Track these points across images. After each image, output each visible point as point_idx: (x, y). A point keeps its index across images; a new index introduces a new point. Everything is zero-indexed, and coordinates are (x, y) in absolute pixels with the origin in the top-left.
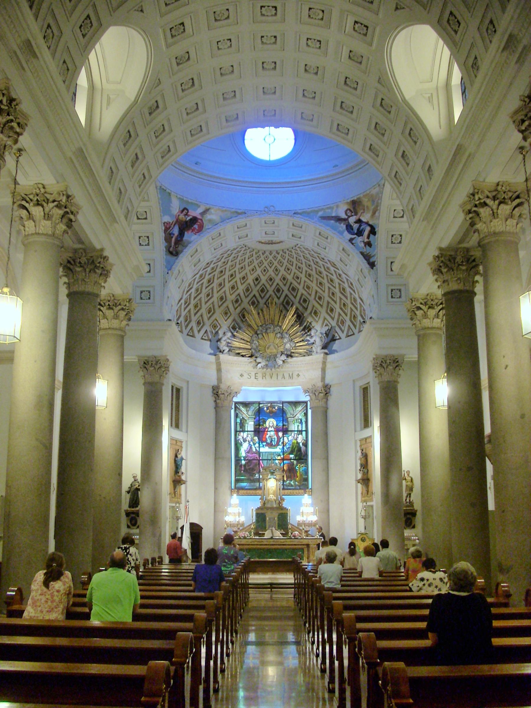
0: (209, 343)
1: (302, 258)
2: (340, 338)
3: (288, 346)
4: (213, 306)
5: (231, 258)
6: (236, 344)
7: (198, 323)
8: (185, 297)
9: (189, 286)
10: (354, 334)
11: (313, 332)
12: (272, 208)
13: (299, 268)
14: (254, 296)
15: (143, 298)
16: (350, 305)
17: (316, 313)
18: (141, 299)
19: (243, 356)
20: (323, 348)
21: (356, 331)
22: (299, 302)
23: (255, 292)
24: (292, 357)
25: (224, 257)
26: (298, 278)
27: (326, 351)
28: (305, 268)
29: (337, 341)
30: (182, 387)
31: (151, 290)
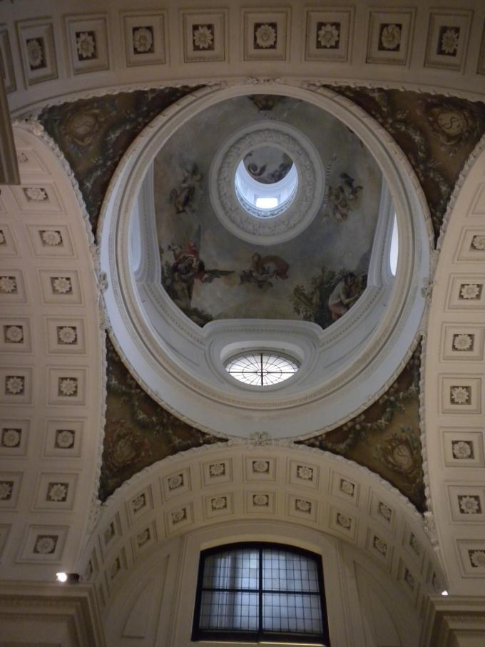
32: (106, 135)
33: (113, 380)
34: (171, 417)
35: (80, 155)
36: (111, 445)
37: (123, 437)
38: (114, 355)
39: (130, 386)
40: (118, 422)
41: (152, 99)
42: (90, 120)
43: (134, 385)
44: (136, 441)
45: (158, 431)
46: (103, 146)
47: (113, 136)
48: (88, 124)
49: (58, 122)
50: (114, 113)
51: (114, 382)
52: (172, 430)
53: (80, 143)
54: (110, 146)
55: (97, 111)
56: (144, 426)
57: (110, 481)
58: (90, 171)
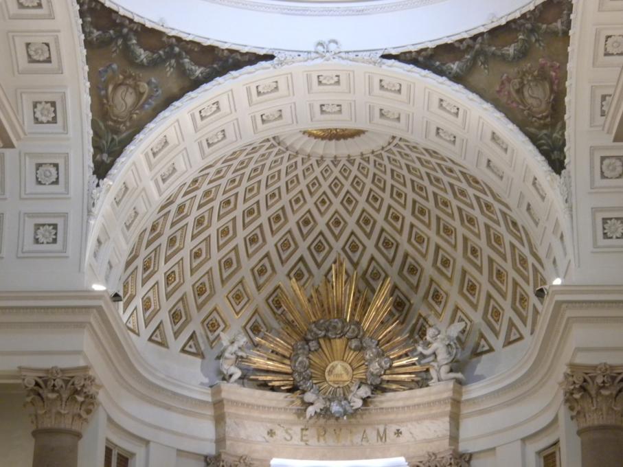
0: (198, 360)
1: (405, 172)
2: (491, 350)
3: (375, 367)
4: (211, 279)
5: (247, 171)
6: (260, 362)
7: (175, 316)
8: (144, 253)
9: (154, 228)
10: (521, 338)
11: (430, 332)
12: (332, 47)
13: (399, 195)
14: (301, 259)
15: (42, 240)
16: (513, 274)
17: (436, 296)
18: (37, 241)
19: (273, 389)
20: (451, 371)
21: (525, 331)
22: (400, 273)
23: (303, 250)
24: (384, 391)
25: (232, 169)
26: (396, 218)
27: (459, 375)
28: (411, 196)
29: (484, 357)
30: (133, 455)
31: (59, 222)
32: (141, 66)
33: (452, 66)
34: (528, 16)
35: (160, 92)
36: (521, 107)
37: (522, 85)
38: (423, 53)
39: (470, 47)
40: (503, 83)
41: (98, 30)
42: (122, 90)
43: (471, 42)
44: (536, 73)
45: (537, 40)
46: (155, 64)
47: (142, 57)
48: (124, 94)
49: (115, 137)
50: (115, 66)
51: (455, 67)
52: (543, 23)
53: (145, 96)
54: (155, 56)
55: (110, 88)
56: (523, 54)
57: (555, 135)
58: (182, 72)
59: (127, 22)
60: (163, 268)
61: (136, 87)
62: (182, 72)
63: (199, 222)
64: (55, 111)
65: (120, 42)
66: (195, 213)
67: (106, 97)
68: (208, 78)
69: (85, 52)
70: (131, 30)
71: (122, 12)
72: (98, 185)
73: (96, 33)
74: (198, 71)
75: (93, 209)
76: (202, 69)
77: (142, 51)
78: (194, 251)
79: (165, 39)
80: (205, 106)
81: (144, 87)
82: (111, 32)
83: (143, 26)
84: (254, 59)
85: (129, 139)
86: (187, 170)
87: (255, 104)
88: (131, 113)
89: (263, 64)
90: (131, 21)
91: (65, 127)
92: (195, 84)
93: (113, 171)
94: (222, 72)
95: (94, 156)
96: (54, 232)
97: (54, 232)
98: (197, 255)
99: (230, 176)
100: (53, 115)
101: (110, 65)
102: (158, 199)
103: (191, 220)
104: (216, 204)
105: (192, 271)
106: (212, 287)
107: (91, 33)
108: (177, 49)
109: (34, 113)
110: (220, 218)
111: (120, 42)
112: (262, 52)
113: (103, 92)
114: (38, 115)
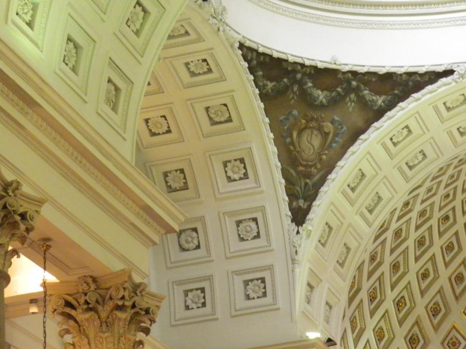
4: (443, 298)
8: (366, 285)
9: (373, 258)
15: (252, 295)
18: (248, 297)
25: (443, 185)
31: (266, 275)
32: (322, 106)
35: (345, 128)
41: (271, 81)
42: (305, 136)
46: (335, 102)
47: (321, 97)
48: (309, 137)
49: (308, 181)
50: (295, 112)
53: (331, 135)
54: (334, 94)
55: (295, 134)
58: (363, 103)
59: (299, 67)
60: (391, 296)
61: (320, 129)
62: (363, 103)
63: (420, 242)
64: (245, 168)
65: (296, 88)
66: (414, 236)
67: (292, 143)
68: (391, 106)
69: (262, 105)
70: (304, 74)
71: (291, 59)
72: (298, 232)
73: (270, 85)
74: (380, 101)
75: (296, 258)
76: (383, 97)
77: (320, 92)
78: (421, 272)
79: (340, 76)
80: (395, 132)
81: (328, 127)
82: (285, 80)
83: (315, 68)
84: (434, 77)
85: (323, 181)
86: (394, 199)
87: (447, 120)
88: (320, 155)
89: (444, 80)
90: (303, 65)
91: (257, 180)
92: (380, 114)
93: (310, 216)
94: (404, 97)
95: (290, 205)
96: (263, 285)
97: (263, 285)
98: (425, 276)
99: (442, 192)
100: (244, 171)
101: (290, 113)
102: (368, 232)
103: (410, 243)
104: (434, 222)
105: (423, 293)
106: (446, 305)
107: (265, 85)
108: (354, 83)
109: (226, 172)
110: (441, 234)
111: (296, 88)
112: (440, 69)
113: (288, 140)
114: (230, 174)
